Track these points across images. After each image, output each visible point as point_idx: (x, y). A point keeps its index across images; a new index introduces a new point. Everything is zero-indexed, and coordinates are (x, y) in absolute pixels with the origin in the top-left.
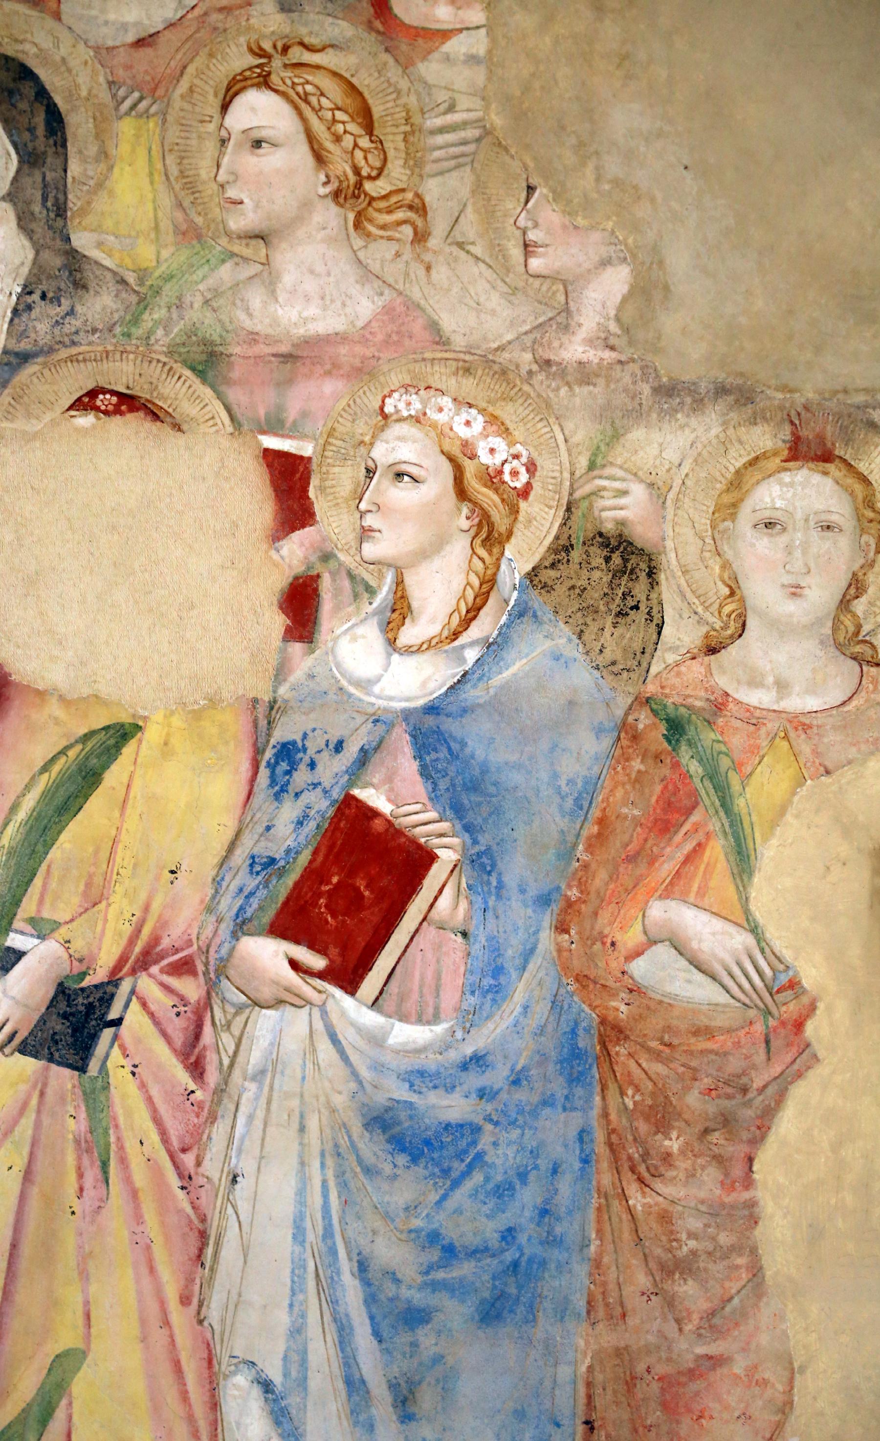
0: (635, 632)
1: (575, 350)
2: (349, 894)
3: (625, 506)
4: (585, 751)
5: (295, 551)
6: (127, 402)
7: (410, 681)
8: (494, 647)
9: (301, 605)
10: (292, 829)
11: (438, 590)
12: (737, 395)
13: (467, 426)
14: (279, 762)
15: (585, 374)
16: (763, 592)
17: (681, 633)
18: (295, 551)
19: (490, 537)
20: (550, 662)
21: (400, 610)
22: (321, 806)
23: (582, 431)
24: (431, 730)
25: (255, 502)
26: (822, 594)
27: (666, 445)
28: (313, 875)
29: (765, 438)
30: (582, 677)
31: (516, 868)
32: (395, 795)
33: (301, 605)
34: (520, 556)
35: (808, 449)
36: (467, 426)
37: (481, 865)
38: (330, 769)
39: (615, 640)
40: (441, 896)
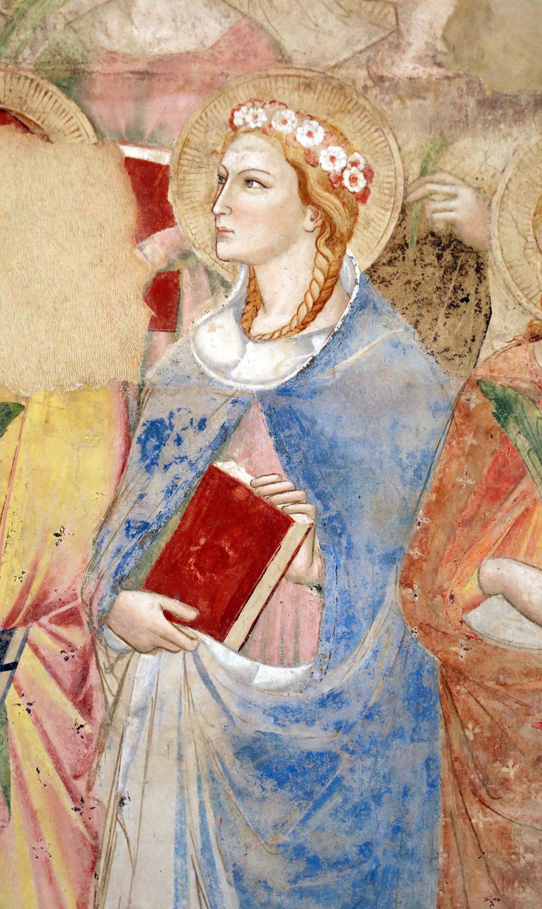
0: (465, 322)
2: (216, 552)
4: (423, 428)
5: (157, 250)
7: (264, 366)
8: (339, 336)
9: (164, 298)
10: (163, 497)
11: (287, 284)
14: (149, 439)
18: (157, 250)
19: (333, 237)
20: (389, 349)
21: (253, 303)
22: (188, 477)
25: (119, 206)
28: (183, 537)
30: (418, 363)
32: (254, 467)
33: (164, 298)
34: (361, 254)
37: (332, 528)
38: (196, 444)
39: (449, 329)
40: (297, 555)
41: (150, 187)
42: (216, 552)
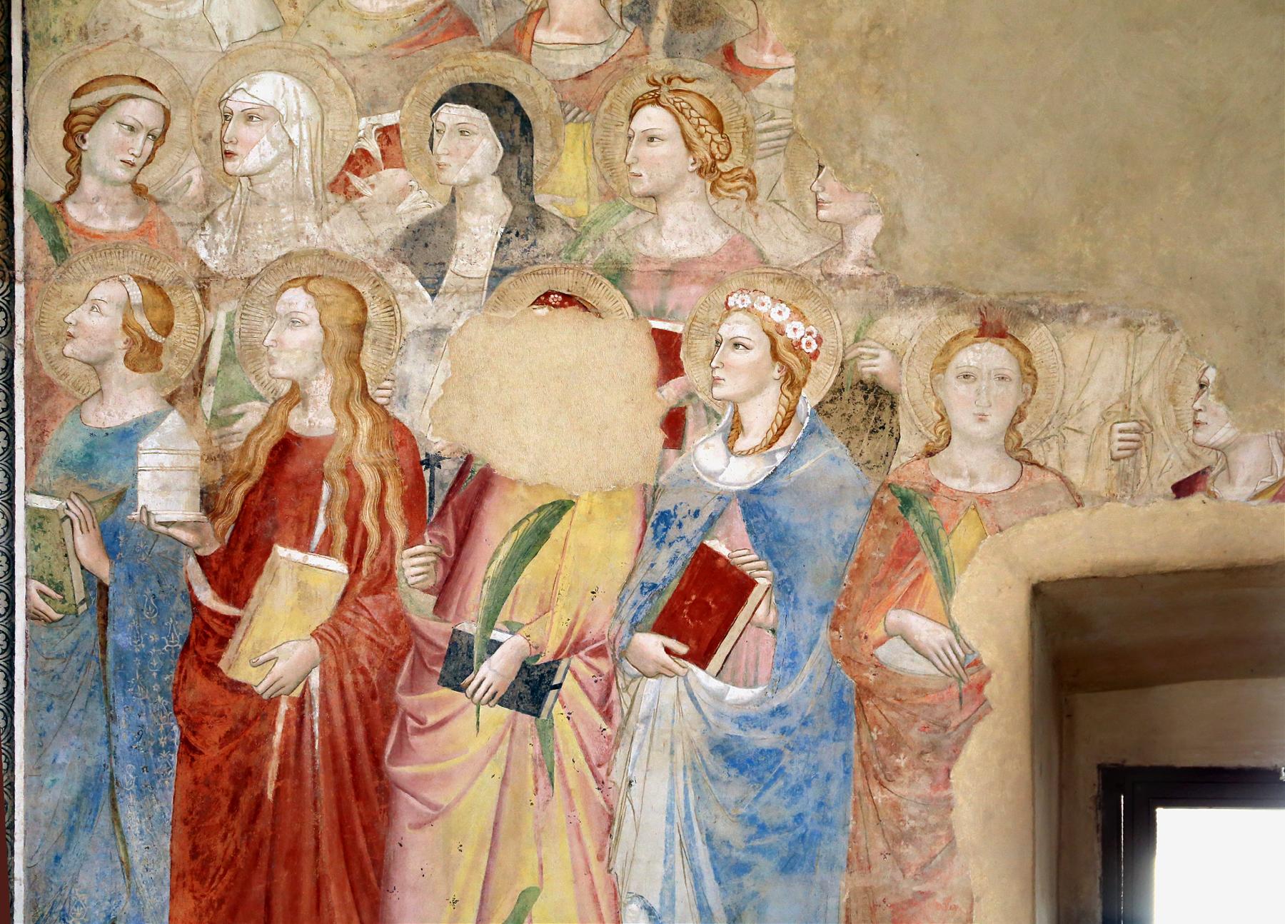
0: (882, 442)
1: (847, 267)
2: (702, 606)
3: (878, 365)
4: (850, 516)
5: (671, 392)
6: (569, 300)
7: (741, 473)
8: (794, 452)
9: (674, 425)
10: (667, 566)
11: (760, 415)
12: (948, 296)
13: (779, 314)
14: (659, 524)
15: (853, 283)
16: (962, 418)
17: (910, 443)
18: (671, 392)
19: (793, 383)
20: (829, 461)
21: (736, 428)
22: (685, 551)
23: (850, 318)
24: (754, 504)
25: (646, 360)
26: (998, 419)
27: (903, 327)
28: (680, 595)
29: (964, 323)
30: (849, 471)
31: (806, 590)
32: (731, 545)
33: (674, 425)
34: (810, 397)
35: (991, 330)
36: (779, 314)
37: (784, 588)
39: (869, 447)
40: (759, 608)
41: (668, 350)
42: (702, 606)
